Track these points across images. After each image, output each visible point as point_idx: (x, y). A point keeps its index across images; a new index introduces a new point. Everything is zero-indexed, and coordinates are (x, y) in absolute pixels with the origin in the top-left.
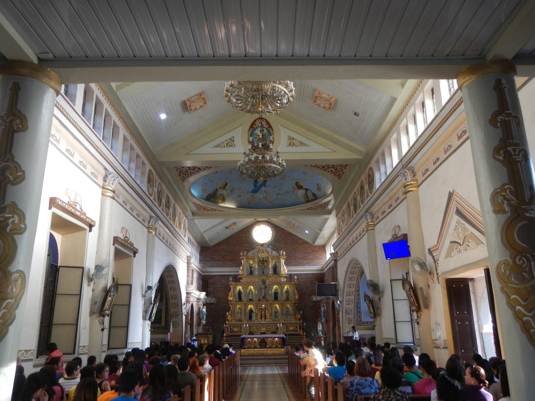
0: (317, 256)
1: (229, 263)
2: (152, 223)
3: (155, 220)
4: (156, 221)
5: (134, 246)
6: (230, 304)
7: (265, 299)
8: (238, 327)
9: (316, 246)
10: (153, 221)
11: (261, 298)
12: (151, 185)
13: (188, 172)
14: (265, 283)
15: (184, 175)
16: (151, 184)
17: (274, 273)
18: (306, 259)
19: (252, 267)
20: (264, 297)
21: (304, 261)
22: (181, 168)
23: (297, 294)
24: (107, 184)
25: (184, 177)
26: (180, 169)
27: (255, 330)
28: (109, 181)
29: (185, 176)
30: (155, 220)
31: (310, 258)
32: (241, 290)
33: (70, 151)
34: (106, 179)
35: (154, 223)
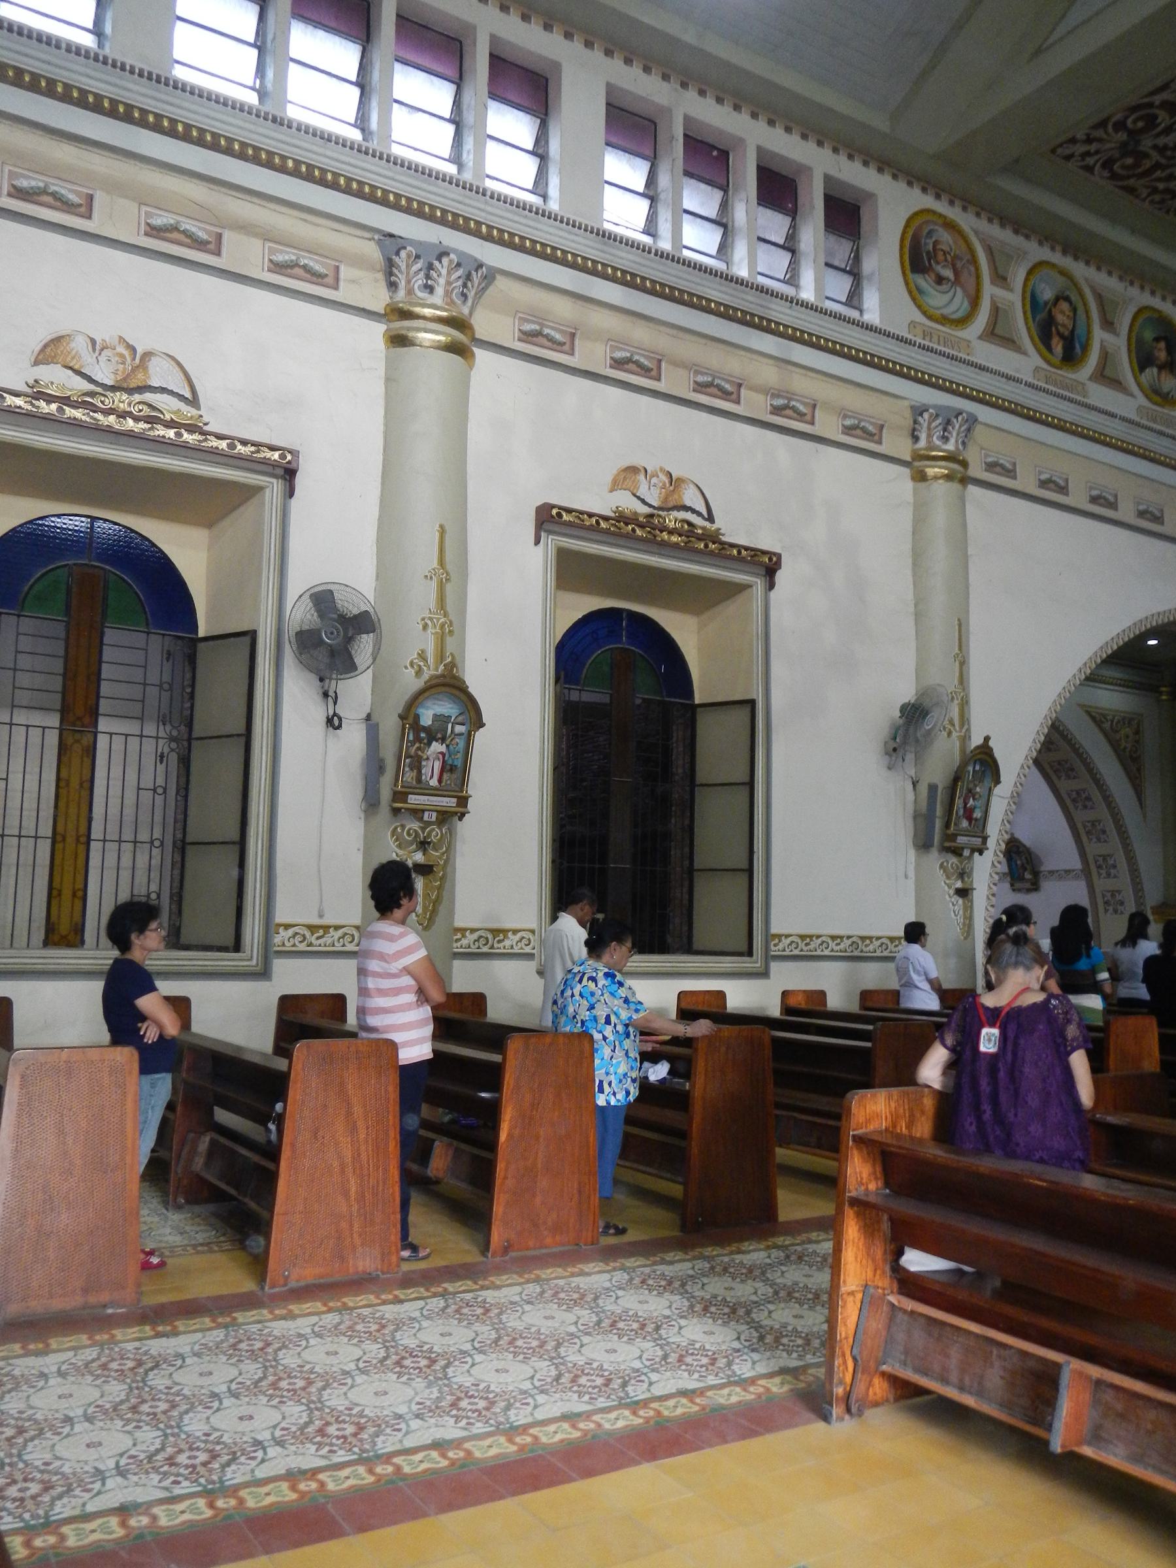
2: (929, 436)
3: (938, 422)
4: (948, 422)
5: (723, 539)
10: (929, 428)
12: (940, 280)
13: (1146, 156)
15: (1142, 181)
16: (948, 273)
22: (1093, 147)
24: (401, 294)
25: (1155, 190)
26: (1088, 154)
28: (408, 282)
29: (1161, 186)
30: (938, 422)
33: (54, 195)
34: (393, 278)
35: (938, 433)
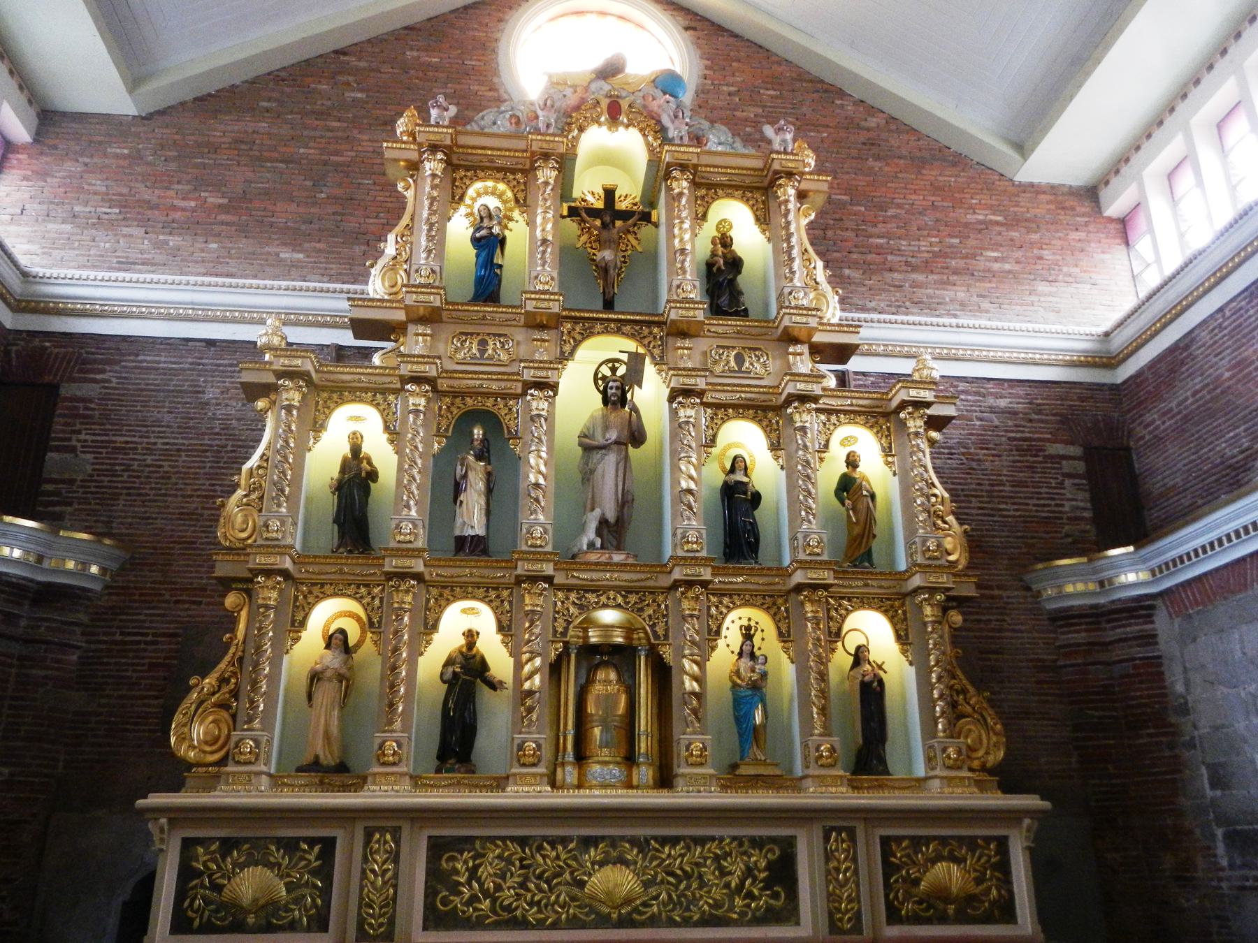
0: (1046, 253)
1: (286, 255)
6: (227, 584)
7: (619, 548)
8: (290, 846)
9: (1033, 190)
11: (590, 534)
14: (623, 401)
17: (716, 310)
18: (955, 272)
19: (502, 242)
20: (612, 532)
21: (944, 284)
23: (950, 518)
27: (507, 895)
31: (996, 266)
32: (366, 449)
